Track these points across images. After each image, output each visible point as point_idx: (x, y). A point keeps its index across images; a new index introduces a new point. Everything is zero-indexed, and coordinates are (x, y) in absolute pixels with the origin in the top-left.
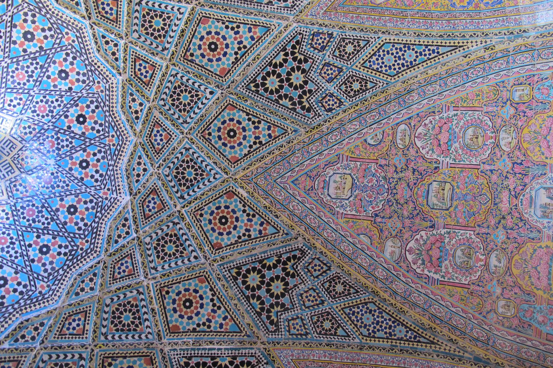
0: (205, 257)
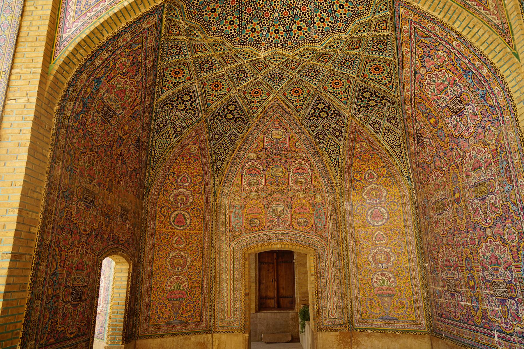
0: (239, 90)
